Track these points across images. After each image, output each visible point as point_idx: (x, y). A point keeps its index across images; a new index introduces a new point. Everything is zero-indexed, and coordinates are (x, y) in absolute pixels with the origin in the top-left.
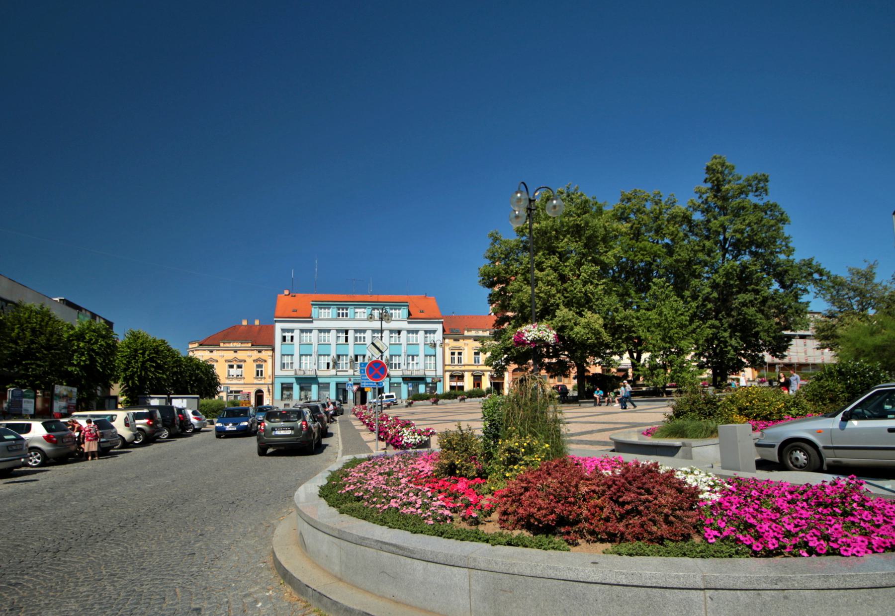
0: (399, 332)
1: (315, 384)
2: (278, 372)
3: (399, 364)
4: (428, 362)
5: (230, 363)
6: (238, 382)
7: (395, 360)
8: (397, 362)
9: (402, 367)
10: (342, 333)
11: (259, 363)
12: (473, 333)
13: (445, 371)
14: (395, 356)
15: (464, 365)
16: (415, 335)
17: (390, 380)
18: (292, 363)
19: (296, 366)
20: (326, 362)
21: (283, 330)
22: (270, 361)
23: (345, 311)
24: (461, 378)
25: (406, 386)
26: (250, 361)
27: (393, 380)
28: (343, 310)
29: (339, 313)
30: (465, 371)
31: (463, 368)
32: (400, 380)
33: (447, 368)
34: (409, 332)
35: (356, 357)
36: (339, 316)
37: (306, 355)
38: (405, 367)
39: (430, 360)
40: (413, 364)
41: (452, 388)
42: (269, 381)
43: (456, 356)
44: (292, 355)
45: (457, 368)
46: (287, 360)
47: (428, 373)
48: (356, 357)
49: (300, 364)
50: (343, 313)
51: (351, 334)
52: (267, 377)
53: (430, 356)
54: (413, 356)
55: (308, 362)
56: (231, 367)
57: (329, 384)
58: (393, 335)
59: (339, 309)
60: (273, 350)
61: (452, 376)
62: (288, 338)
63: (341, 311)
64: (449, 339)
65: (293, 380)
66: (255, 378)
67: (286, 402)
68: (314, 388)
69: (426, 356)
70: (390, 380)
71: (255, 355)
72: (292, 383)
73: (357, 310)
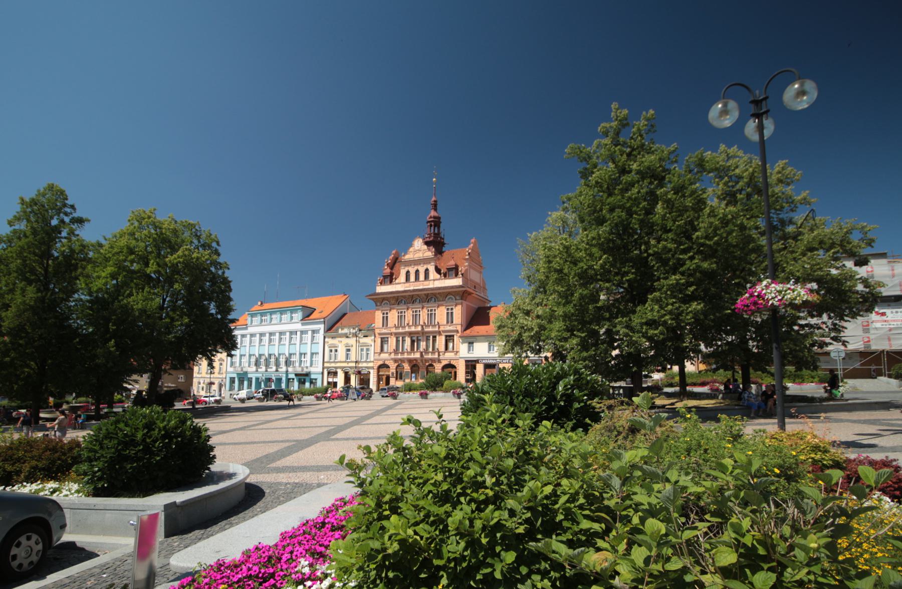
12: (346, 331)
13: (323, 369)
19: (238, 364)
24: (335, 374)
30: (336, 368)
33: (326, 365)
35: (270, 355)
41: (329, 383)
45: (333, 365)
49: (240, 364)
54: (305, 354)
61: (329, 373)
65: (235, 375)
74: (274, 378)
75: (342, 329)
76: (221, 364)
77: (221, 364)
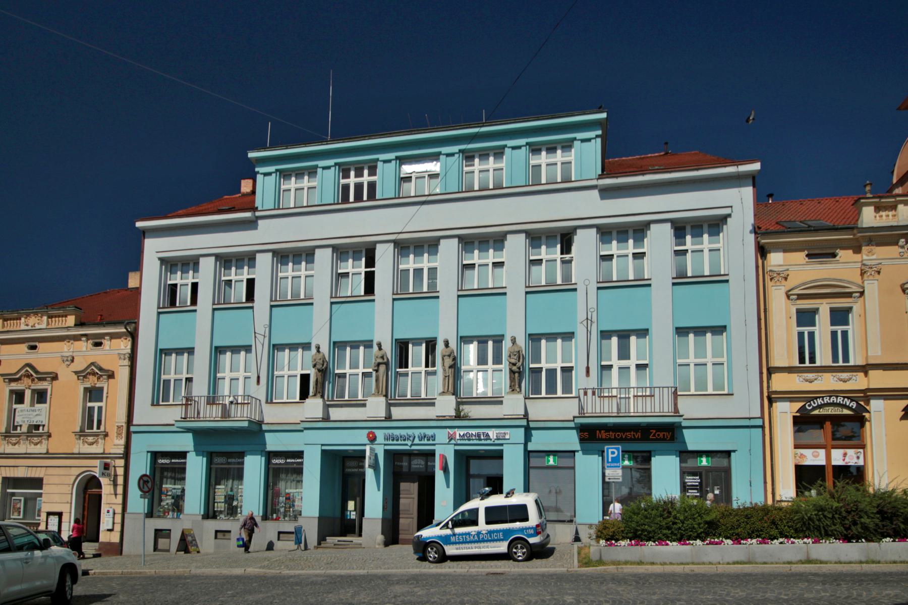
0: (566, 240)
1: (254, 453)
2: (144, 413)
3: (567, 370)
4: (692, 359)
5: (15, 386)
6: (32, 449)
7: (551, 358)
8: (558, 365)
9: (579, 380)
10: (356, 258)
11: (91, 381)
14: (551, 337)
15: (864, 369)
16: (630, 247)
17: (528, 438)
18: (189, 380)
19: (200, 389)
20: (299, 372)
21: (170, 264)
22: (123, 374)
23: (366, 179)
25: (596, 460)
26: (66, 375)
27: (539, 441)
28: (359, 174)
29: (346, 188)
30: (868, 395)
31: (859, 382)
32: (571, 440)
33: (780, 383)
34: (606, 233)
35: (402, 347)
36: (345, 199)
37: (235, 350)
38: (592, 382)
39: (700, 351)
40: (624, 370)
42: (116, 445)
43: (823, 328)
44: (191, 351)
45: (828, 382)
46: (175, 369)
47: (690, 409)
48: (402, 347)
49: (214, 382)
50: (359, 187)
51: (384, 255)
52: (113, 432)
53: (700, 331)
55: (241, 374)
56: (19, 397)
57: (300, 454)
58: (544, 253)
59: (346, 176)
60: (133, 336)
61: (802, 422)
62: (185, 293)
63: (352, 180)
64: (787, 249)
65: (185, 442)
66: (81, 434)
67: (161, 524)
68: (253, 466)
69: (681, 331)
70: (528, 438)
71: (85, 354)
72: (183, 455)
73: (407, 169)
74: (445, 451)
75: (878, 209)
76: (94, 394)
77: (94, 394)
